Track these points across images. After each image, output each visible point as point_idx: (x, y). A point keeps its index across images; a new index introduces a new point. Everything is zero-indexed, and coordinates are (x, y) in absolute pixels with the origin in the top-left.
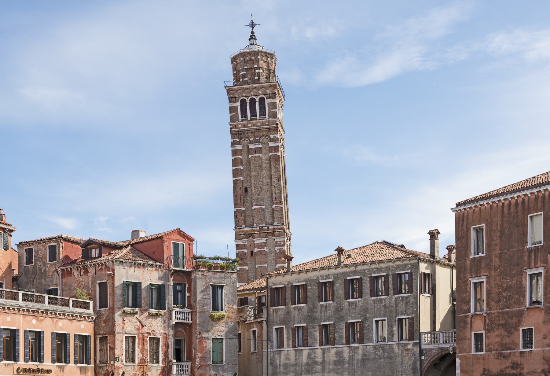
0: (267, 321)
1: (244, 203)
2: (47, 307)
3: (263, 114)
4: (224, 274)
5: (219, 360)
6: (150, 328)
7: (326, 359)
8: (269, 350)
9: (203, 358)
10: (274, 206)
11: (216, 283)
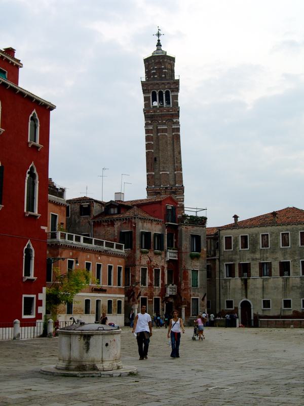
0: (219, 259)
1: (154, 169)
3: (168, 103)
7: (265, 285)
8: (221, 278)
10: (176, 172)
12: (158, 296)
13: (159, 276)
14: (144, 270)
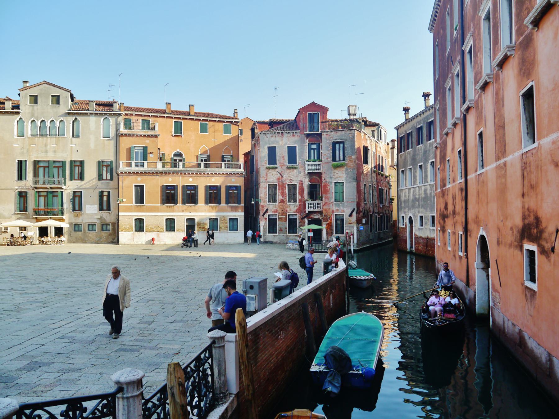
5: (341, 199)
12: (294, 212)
13: (296, 192)
14: (272, 188)
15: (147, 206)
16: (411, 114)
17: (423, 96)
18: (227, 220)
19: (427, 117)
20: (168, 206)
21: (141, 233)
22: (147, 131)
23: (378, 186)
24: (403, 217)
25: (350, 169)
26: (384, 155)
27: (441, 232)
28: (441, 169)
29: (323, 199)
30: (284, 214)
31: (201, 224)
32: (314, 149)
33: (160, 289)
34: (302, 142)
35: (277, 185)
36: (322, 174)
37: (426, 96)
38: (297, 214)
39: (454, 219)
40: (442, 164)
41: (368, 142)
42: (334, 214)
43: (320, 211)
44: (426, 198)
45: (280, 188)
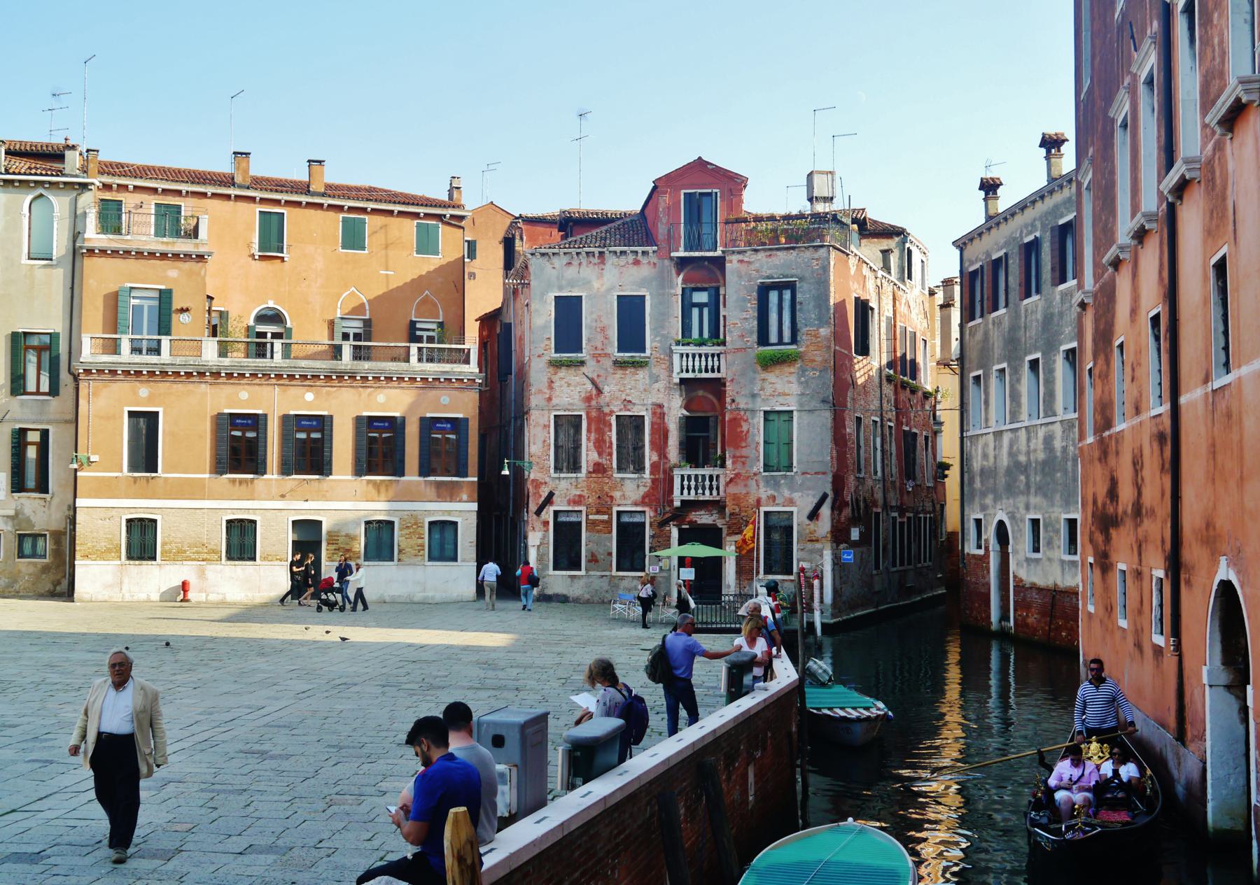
2: (346, 365)
4: (794, 253)
5: (784, 462)
6: (618, 394)
9: (739, 459)
11: (773, 278)
12: (636, 504)
13: (643, 440)
14: (567, 426)
15: (166, 479)
16: (1006, 199)
17: (1041, 146)
18: (423, 527)
19: (1056, 211)
20: (234, 481)
21: (146, 566)
22: (171, 240)
23: (899, 423)
24: (978, 522)
25: (813, 369)
26: (919, 326)
27: (1098, 572)
28: (1096, 372)
29: (729, 463)
30: (605, 510)
31: (341, 539)
32: (701, 306)
33: (204, 746)
34: (663, 283)
35: (584, 417)
36: (724, 385)
37: (1051, 144)
38: (647, 509)
39: (1140, 530)
40: (1101, 361)
41: (871, 285)
42: (763, 509)
43: (718, 501)
44: (1049, 465)
45: (593, 427)
